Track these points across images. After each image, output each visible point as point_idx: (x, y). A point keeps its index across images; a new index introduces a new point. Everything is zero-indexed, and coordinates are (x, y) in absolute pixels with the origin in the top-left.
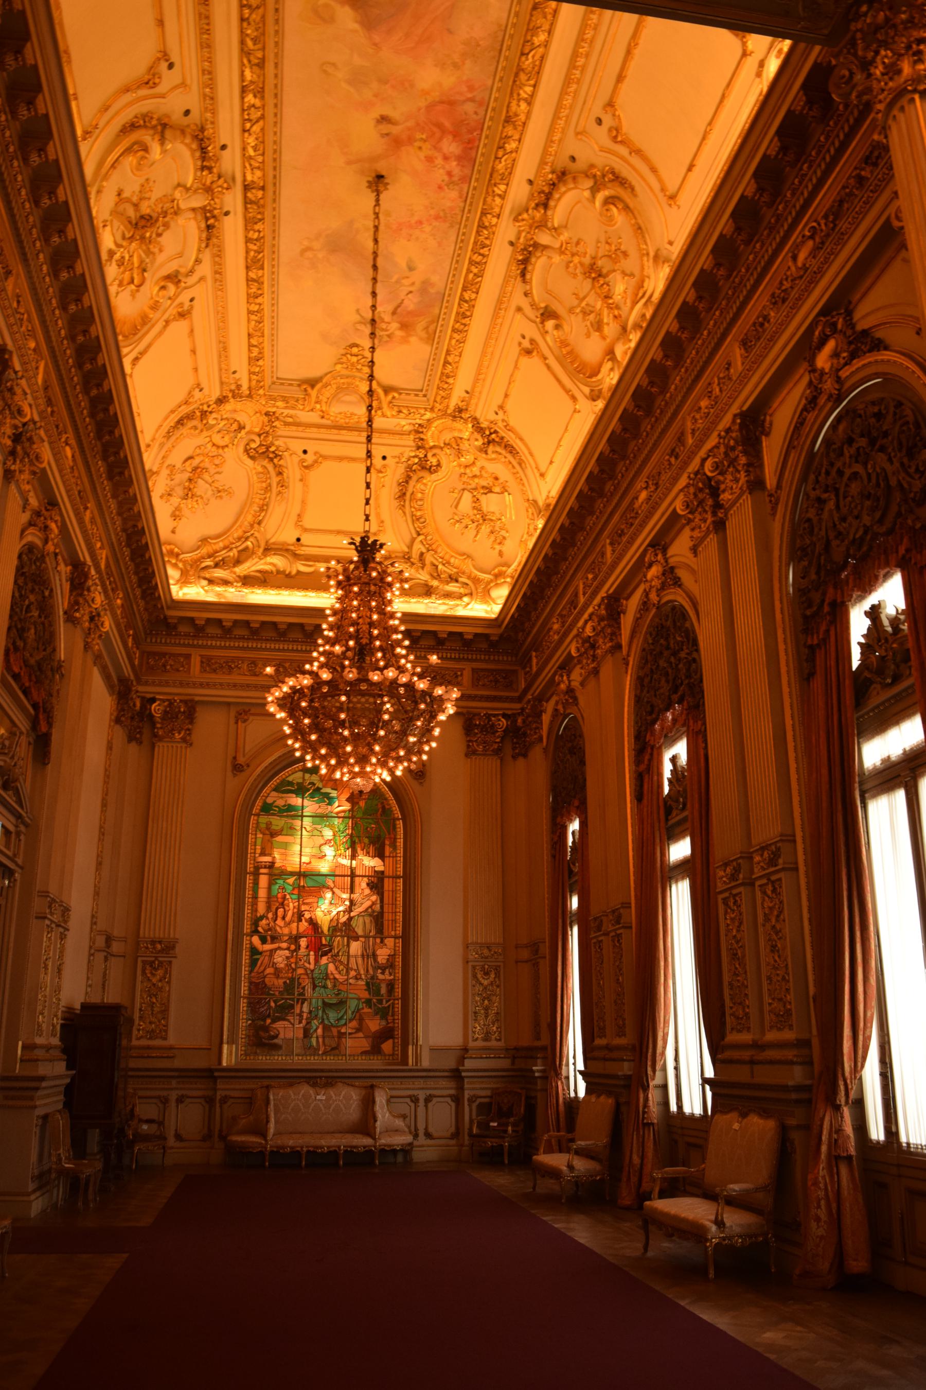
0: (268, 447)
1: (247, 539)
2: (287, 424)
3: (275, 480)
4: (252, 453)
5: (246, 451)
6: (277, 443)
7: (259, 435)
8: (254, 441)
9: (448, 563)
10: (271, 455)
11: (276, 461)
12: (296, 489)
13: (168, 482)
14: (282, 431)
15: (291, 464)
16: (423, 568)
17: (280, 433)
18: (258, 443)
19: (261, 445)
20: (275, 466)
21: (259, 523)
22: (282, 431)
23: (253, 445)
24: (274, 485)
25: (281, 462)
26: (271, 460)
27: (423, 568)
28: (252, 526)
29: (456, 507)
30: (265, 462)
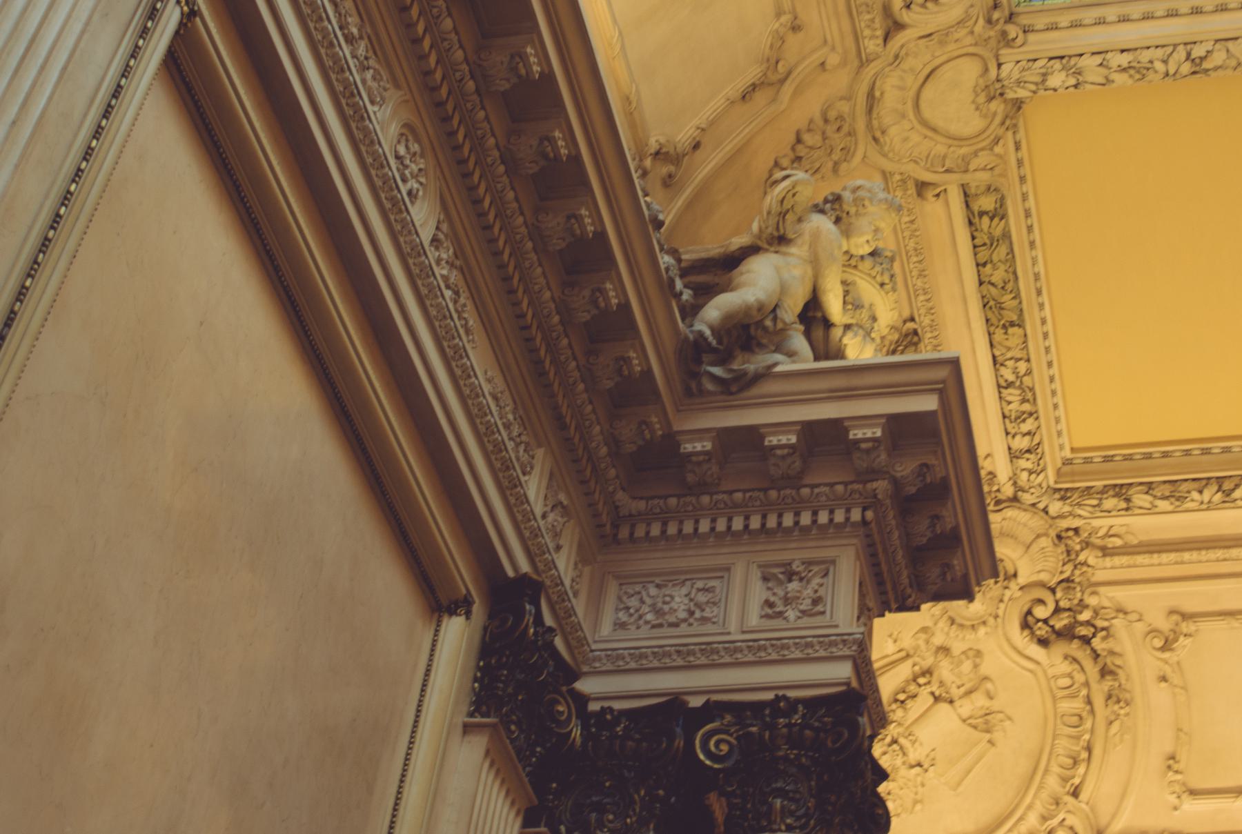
2: (1106, 552)
3: (1099, 691)
4: (1042, 630)
6: (1092, 601)
7: (1053, 591)
8: (1041, 602)
11: (1096, 643)
12: (1155, 704)
14: (1102, 568)
15: (1127, 643)
17: (1100, 576)
18: (1051, 607)
19: (1057, 610)
20: (1096, 655)
22: (1102, 568)
23: (1041, 612)
24: (1098, 701)
26: (1086, 641)
30: (1074, 648)
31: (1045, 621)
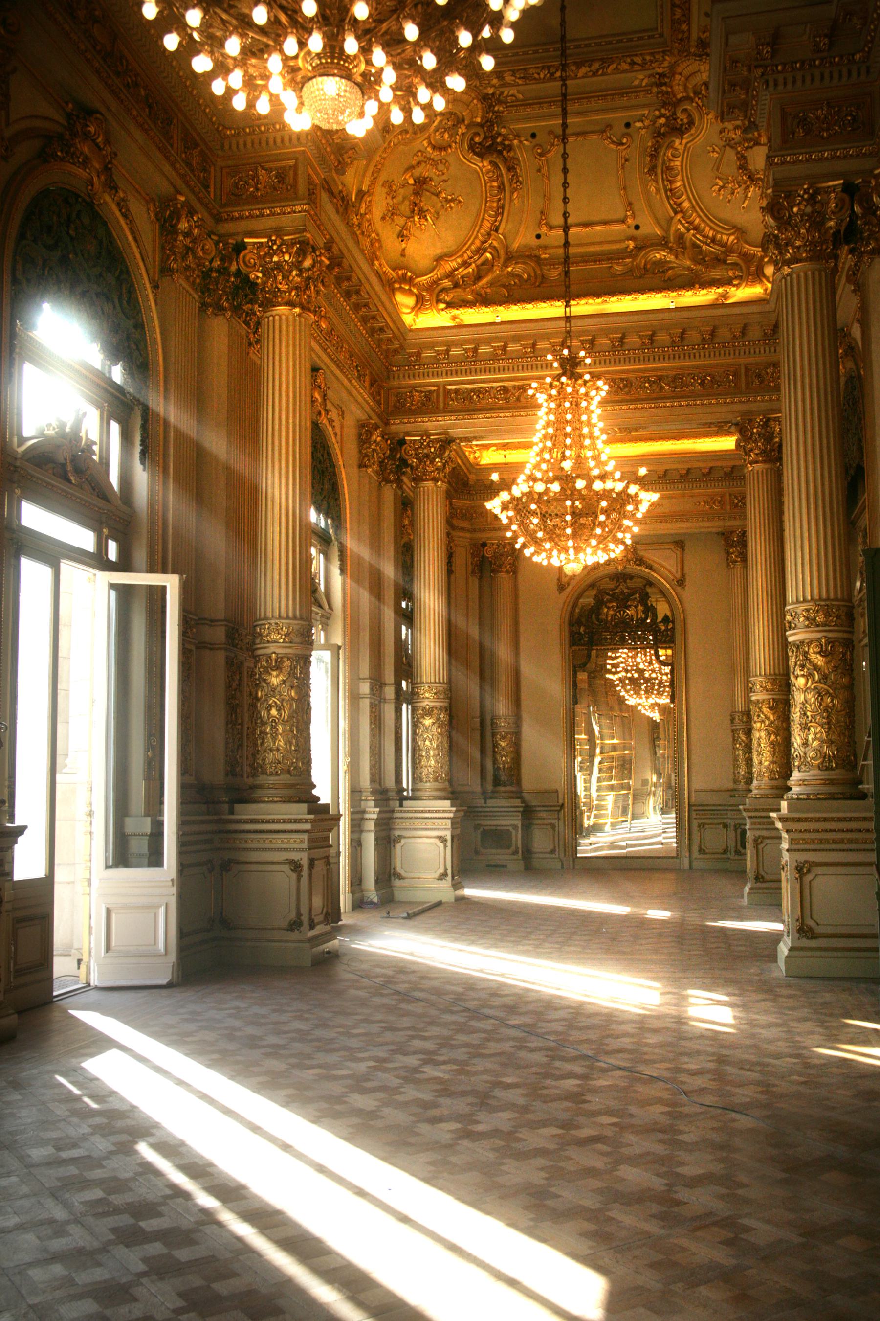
0: (494, 138)
1: (485, 251)
5: (472, 148)
9: (713, 240)
10: (499, 148)
11: (505, 153)
13: (389, 200)
16: (683, 253)
18: (482, 136)
20: (505, 160)
21: (497, 231)
23: (477, 140)
25: (512, 154)
26: (500, 153)
27: (683, 253)
28: (489, 234)
29: (718, 170)
30: (494, 158)
31: (480, 144)
